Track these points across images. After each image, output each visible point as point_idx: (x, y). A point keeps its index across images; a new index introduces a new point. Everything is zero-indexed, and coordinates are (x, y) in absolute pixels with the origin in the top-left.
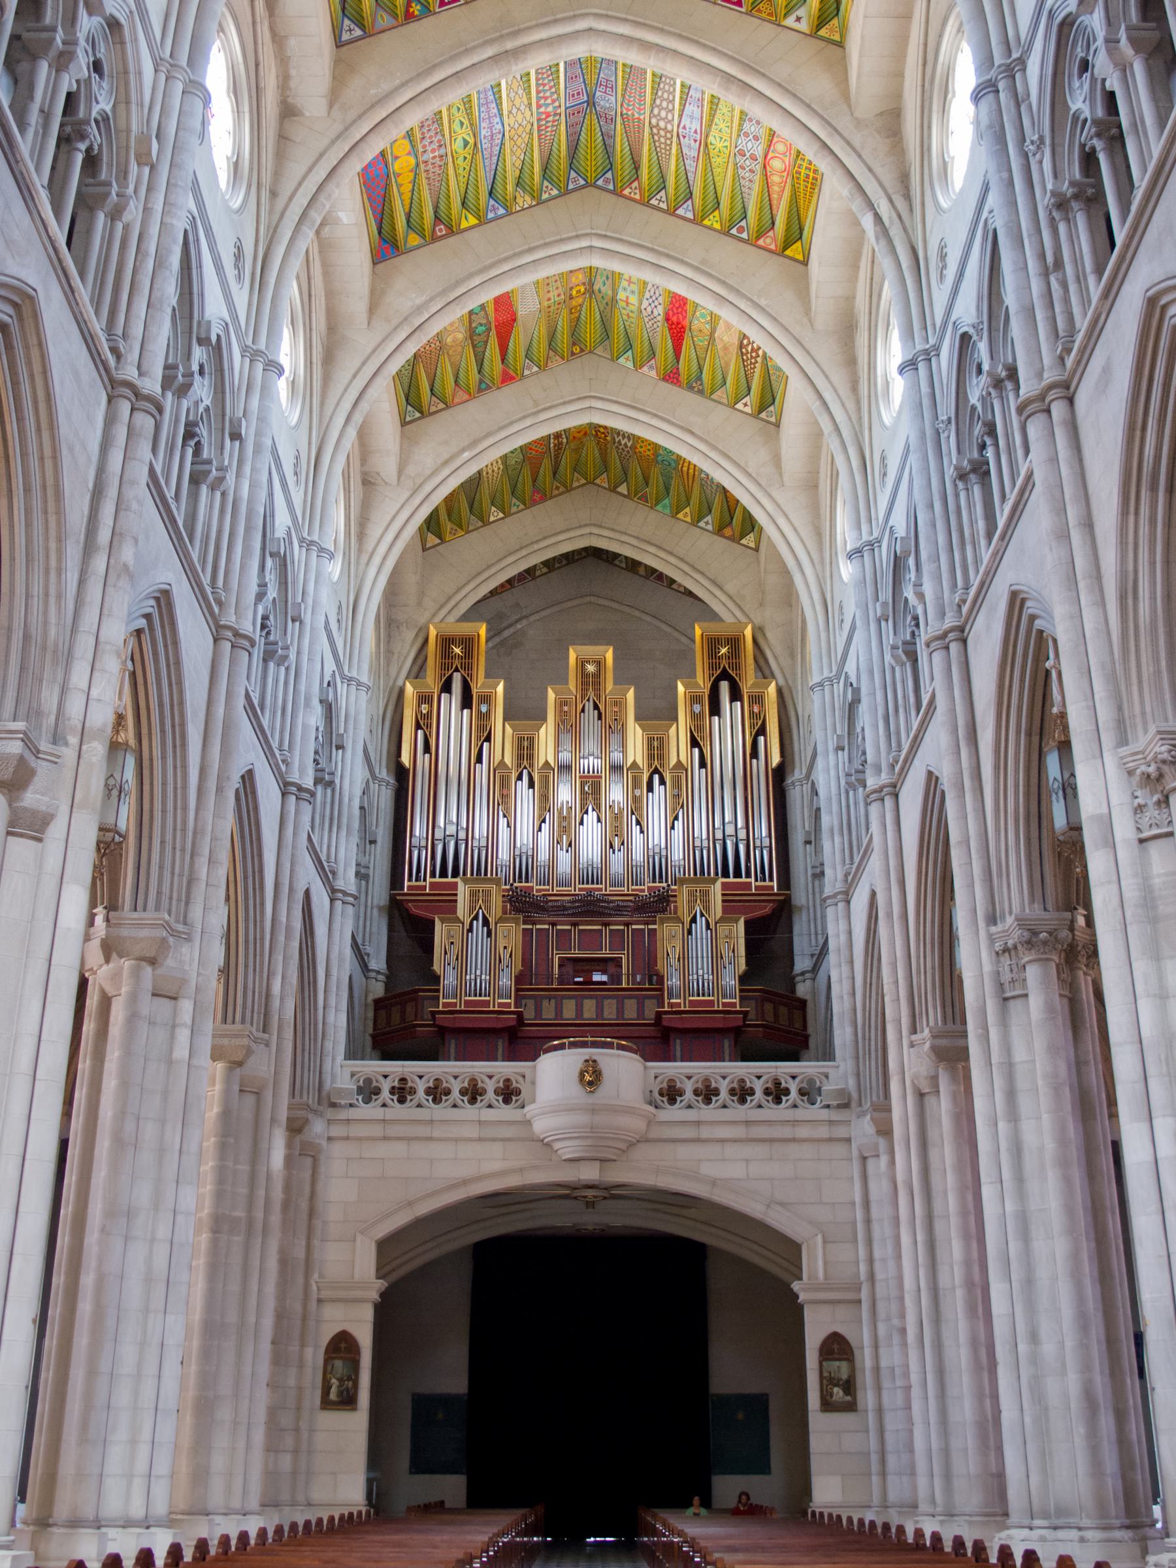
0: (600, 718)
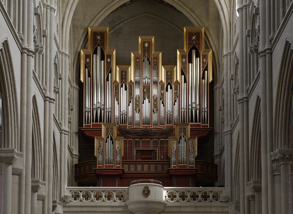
0: (150, 64)
